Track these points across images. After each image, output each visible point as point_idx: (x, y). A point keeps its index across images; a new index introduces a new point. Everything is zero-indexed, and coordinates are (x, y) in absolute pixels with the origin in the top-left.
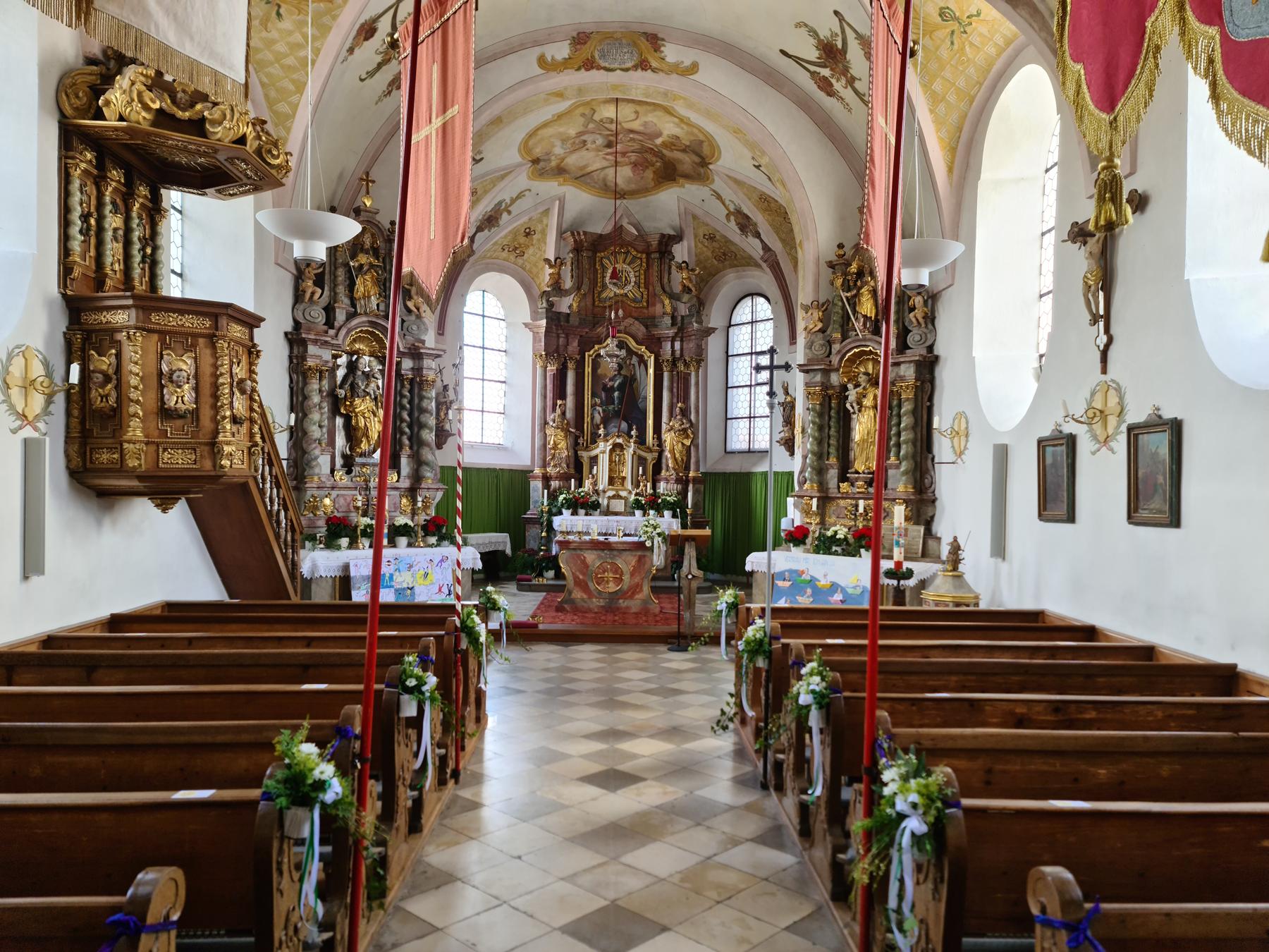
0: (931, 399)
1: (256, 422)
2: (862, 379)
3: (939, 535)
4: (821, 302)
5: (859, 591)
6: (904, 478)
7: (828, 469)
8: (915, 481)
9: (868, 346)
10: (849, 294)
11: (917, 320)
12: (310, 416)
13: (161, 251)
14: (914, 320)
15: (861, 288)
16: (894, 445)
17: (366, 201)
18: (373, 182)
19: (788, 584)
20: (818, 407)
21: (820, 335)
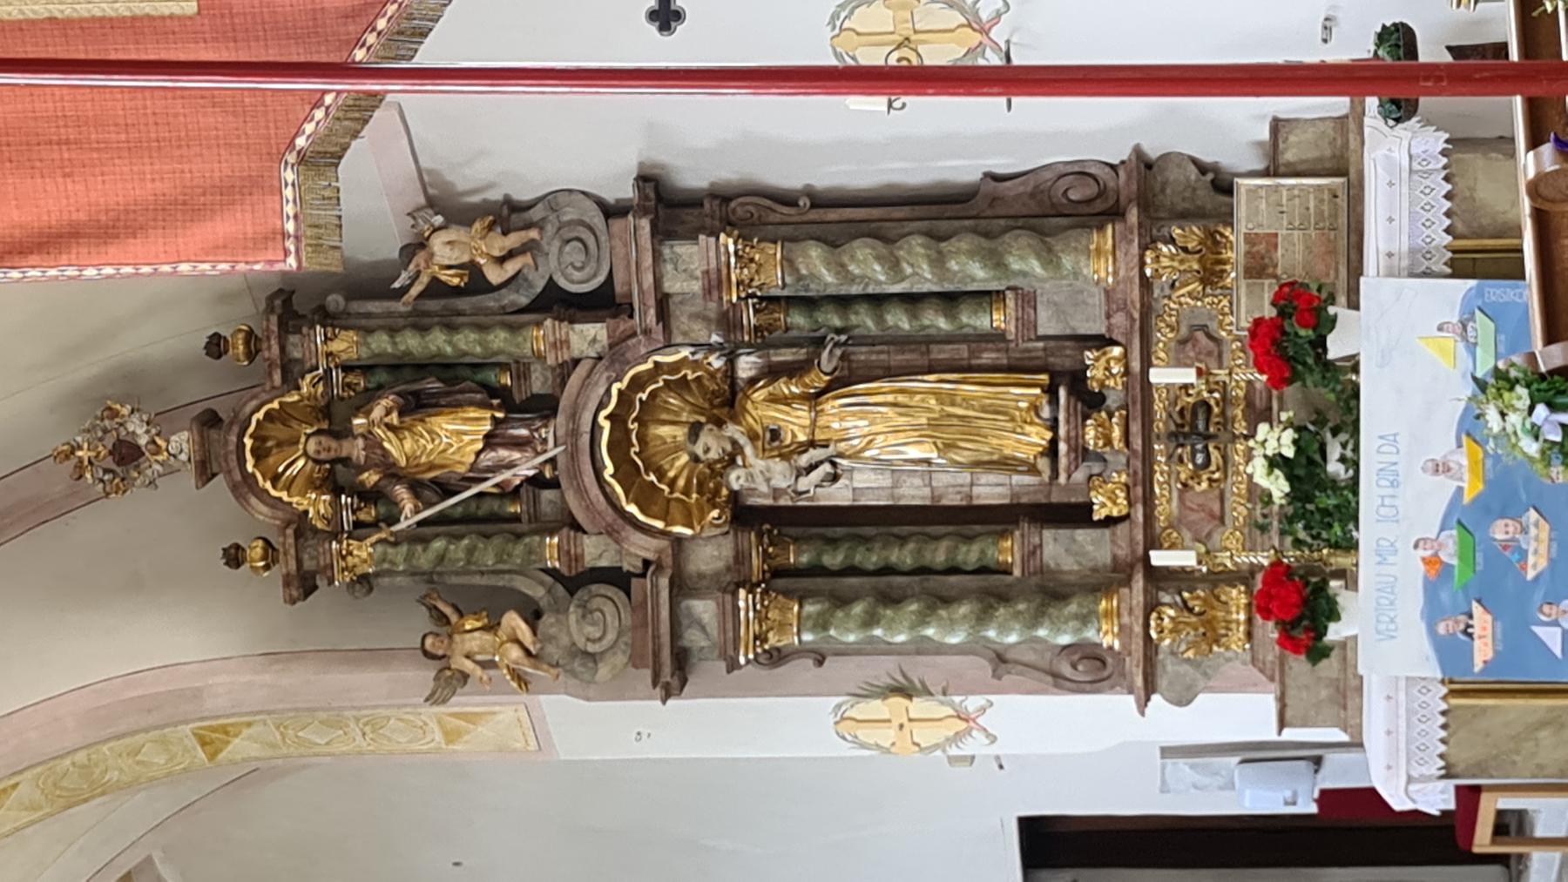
0: (786, 199)
2: (711, 445)
3: (1265, 134)
4: (430, 627)
5: (1483, 327)
6: (1067, 261)
7: (1042, 570)
8: (1083, 226)
9: (595, 428)
10: (408, 507)
11: (511, 255)
14: (511, 267)
15: (392, 473)
16: (951, 315)
19: (1482, 620)
20: (811, 608)
21: (547, 620)
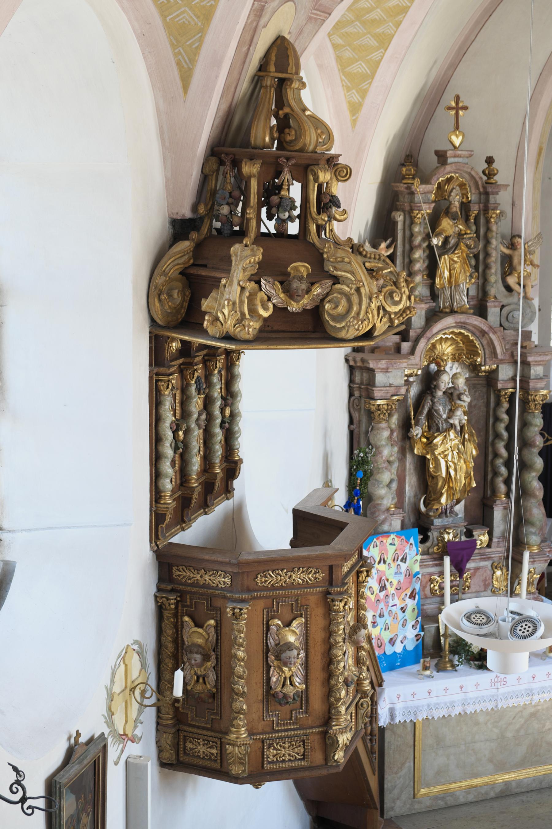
1: (364, 664)
12: (378, 477)
13: (239, 418)
17: (454, 138)
18: (465, 108)
